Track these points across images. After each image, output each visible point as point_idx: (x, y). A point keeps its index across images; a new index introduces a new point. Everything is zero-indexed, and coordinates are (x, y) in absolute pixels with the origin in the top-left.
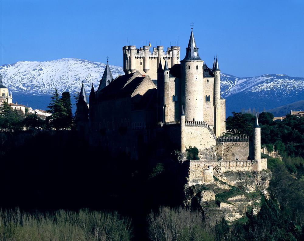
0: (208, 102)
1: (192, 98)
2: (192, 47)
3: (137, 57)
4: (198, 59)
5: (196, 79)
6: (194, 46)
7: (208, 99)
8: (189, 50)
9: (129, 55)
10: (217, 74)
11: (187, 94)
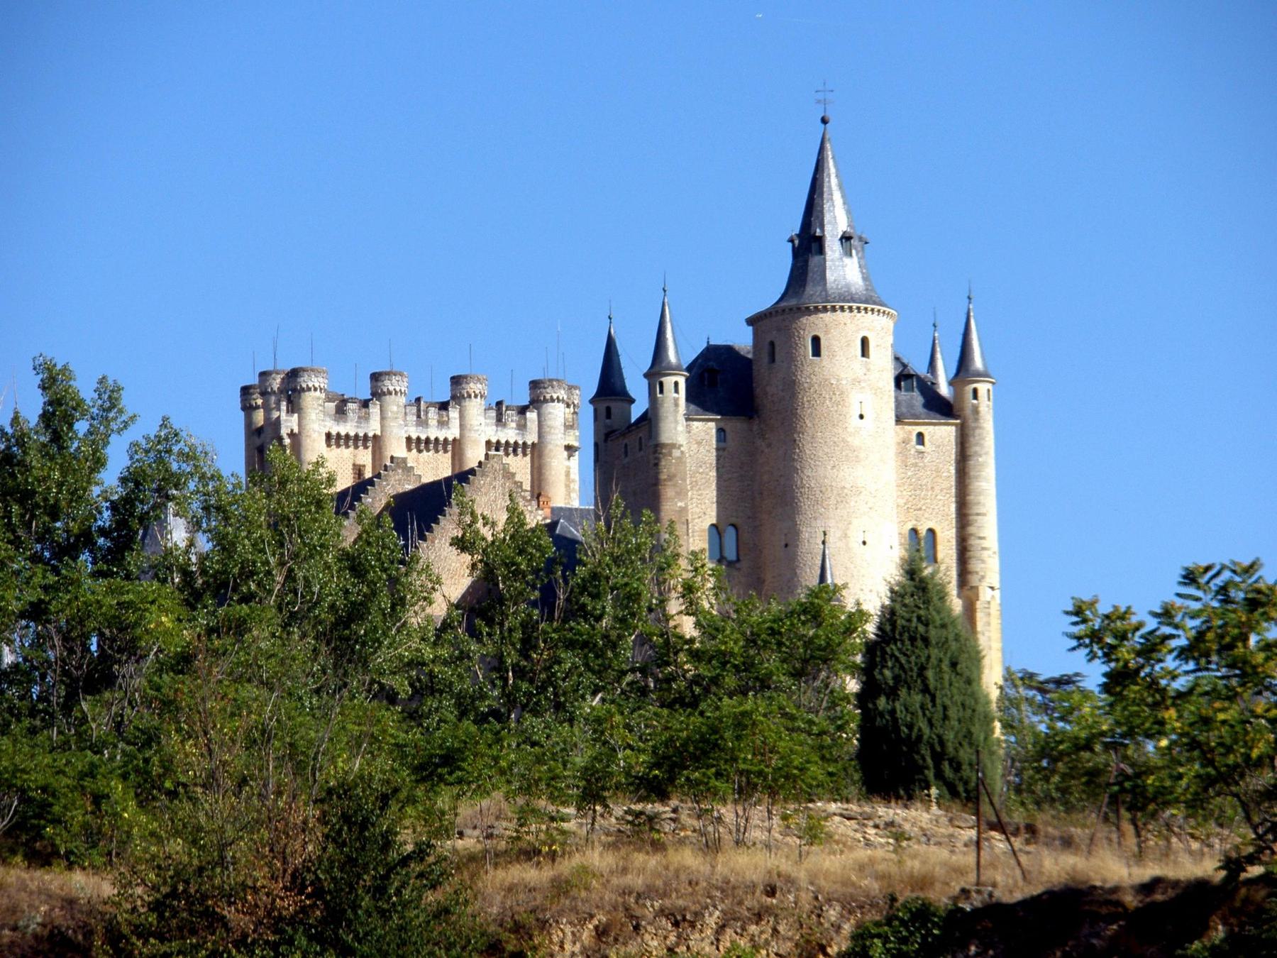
1: (838, 534)
2: (828, 228)
3: (334, 433)
4: (868, 300)
5: (861, 417)
6: (836, 219)
8: (808, 245)
9: (289, 423)
11: (805, 504)
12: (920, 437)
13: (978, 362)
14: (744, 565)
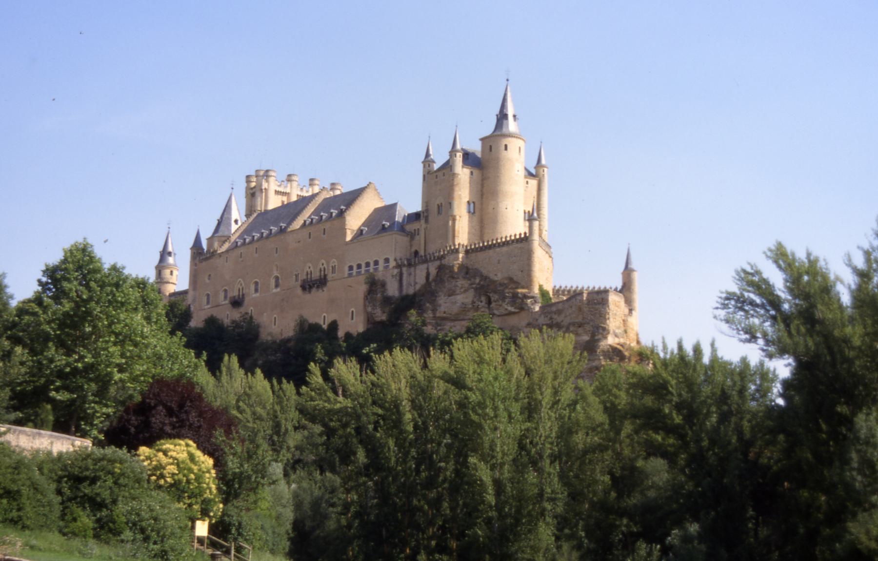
6: (510, 112)
8: (502, 117)
9: (265, 185)
13: (543, 162)
14: (477, 214)
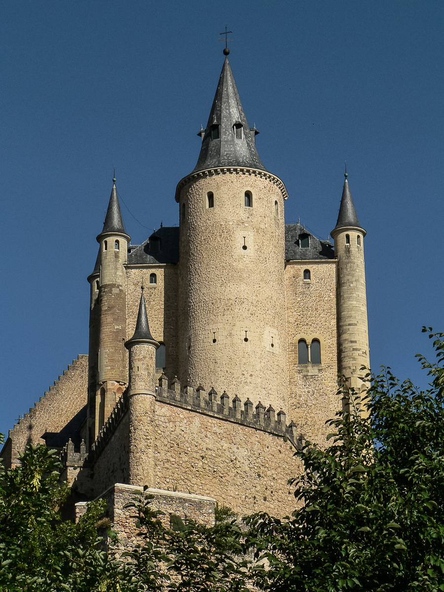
0: (312, 370)
2: (224, 120)
5: (245, 248)
7: (307, 352)
10: (348, 242)
12: (307, 272)
